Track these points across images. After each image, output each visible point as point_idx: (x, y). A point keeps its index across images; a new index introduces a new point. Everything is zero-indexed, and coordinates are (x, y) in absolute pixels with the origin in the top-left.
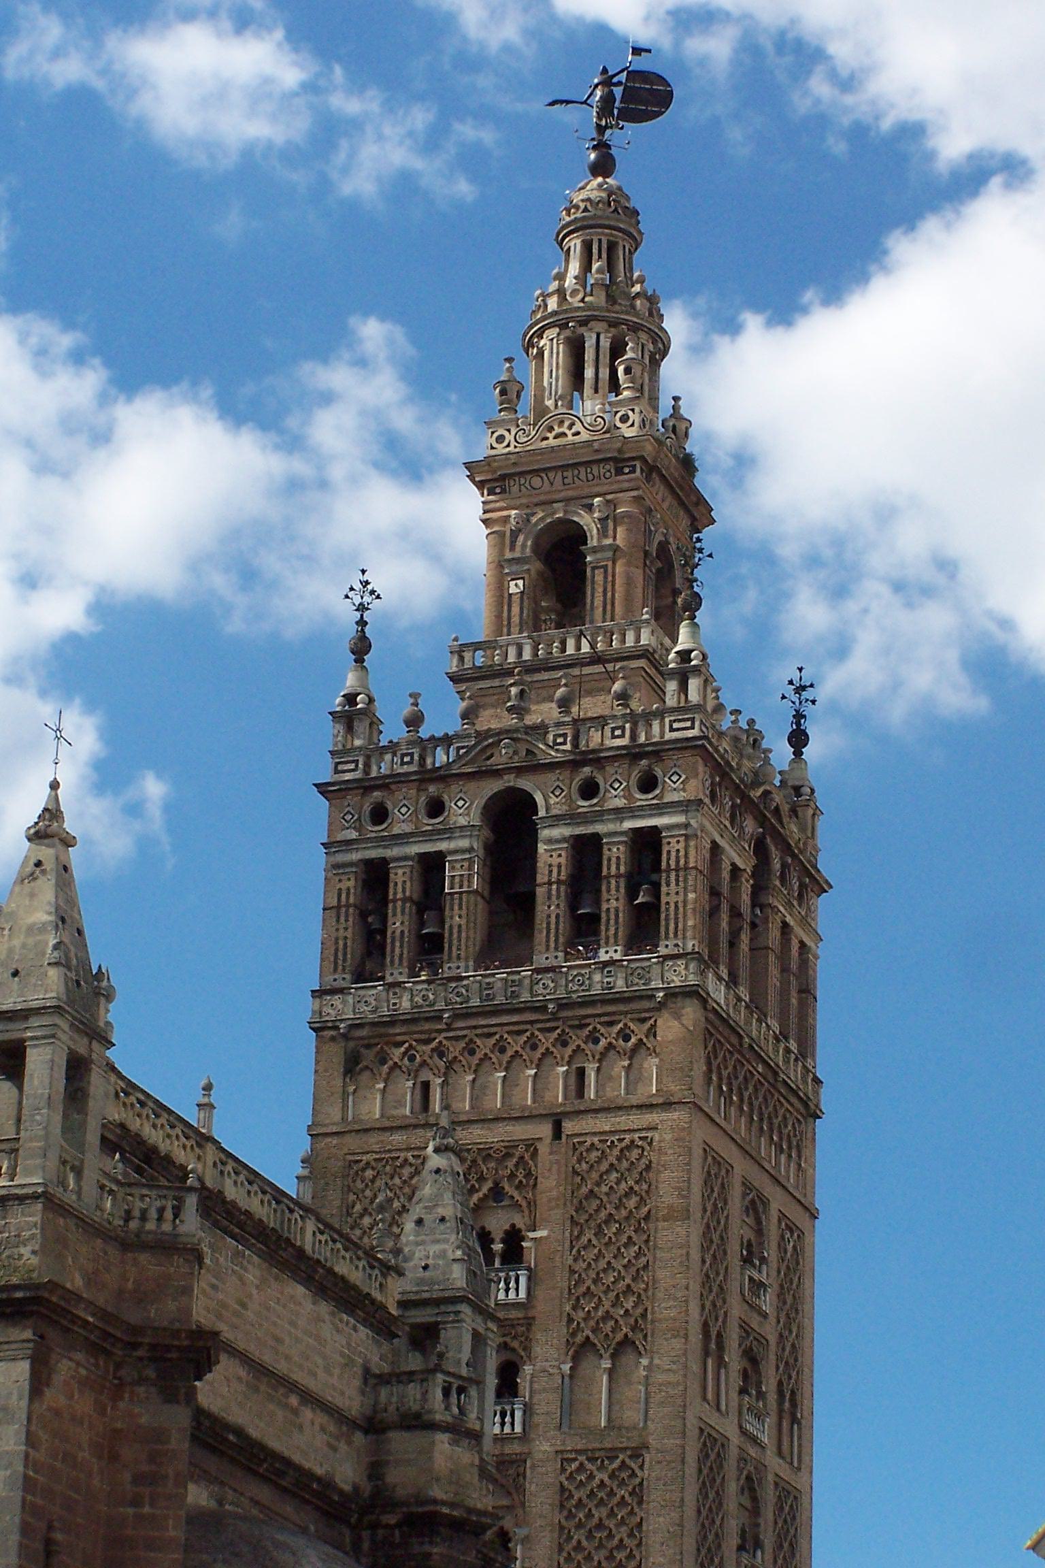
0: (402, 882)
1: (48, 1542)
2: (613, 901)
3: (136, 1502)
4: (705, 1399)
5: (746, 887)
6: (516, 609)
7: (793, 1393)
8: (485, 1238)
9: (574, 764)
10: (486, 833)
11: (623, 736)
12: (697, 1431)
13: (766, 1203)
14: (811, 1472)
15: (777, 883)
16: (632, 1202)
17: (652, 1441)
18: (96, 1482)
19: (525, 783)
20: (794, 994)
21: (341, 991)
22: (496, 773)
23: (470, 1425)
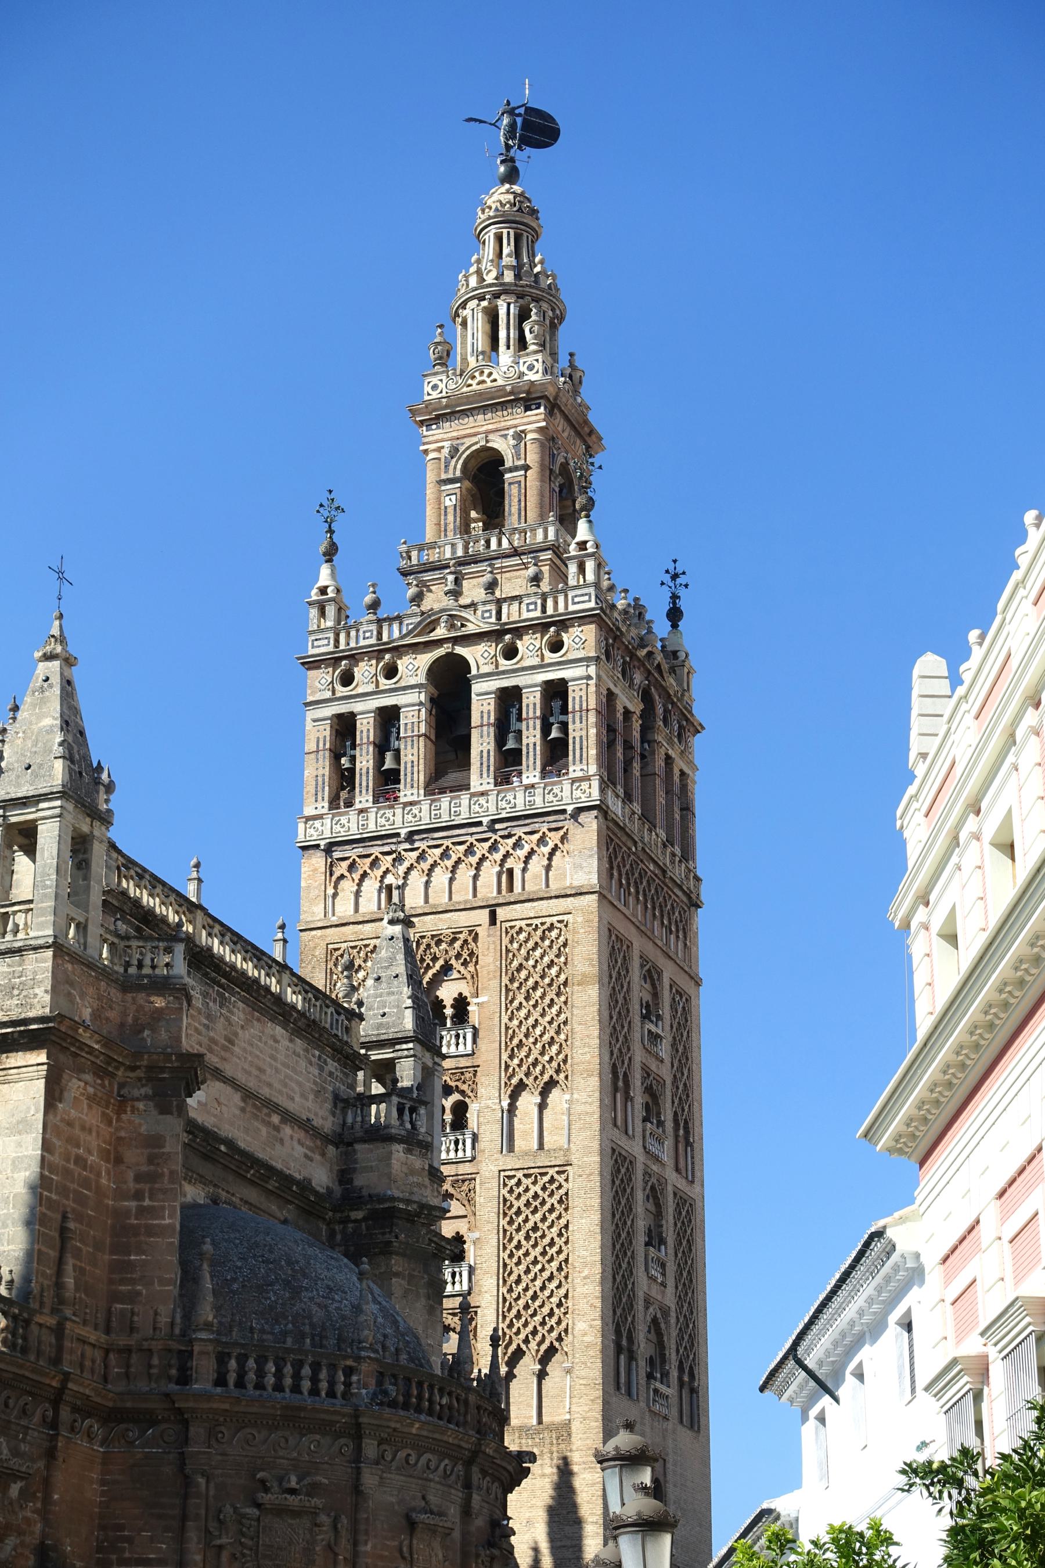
1: (63, 1231)
2: (532, 737)
3: (138, 1196)
4: (615, 1125)
5: (636, 725)
6: (450, 518)
7: (686, 1122)
8: (439, 1005)
10: (432, 689)
11: (536, 609)
12: (610, 1150)
13: (660, 974)
14: (703, 1186)
15: (661, 723)
16: (554, 971)
17: (574, 1159)
18: (104, 1181)
19: (459, 650)
20: (677, 810)
21: (320, 817)
22: (439, 643)
23: (421, 1137)
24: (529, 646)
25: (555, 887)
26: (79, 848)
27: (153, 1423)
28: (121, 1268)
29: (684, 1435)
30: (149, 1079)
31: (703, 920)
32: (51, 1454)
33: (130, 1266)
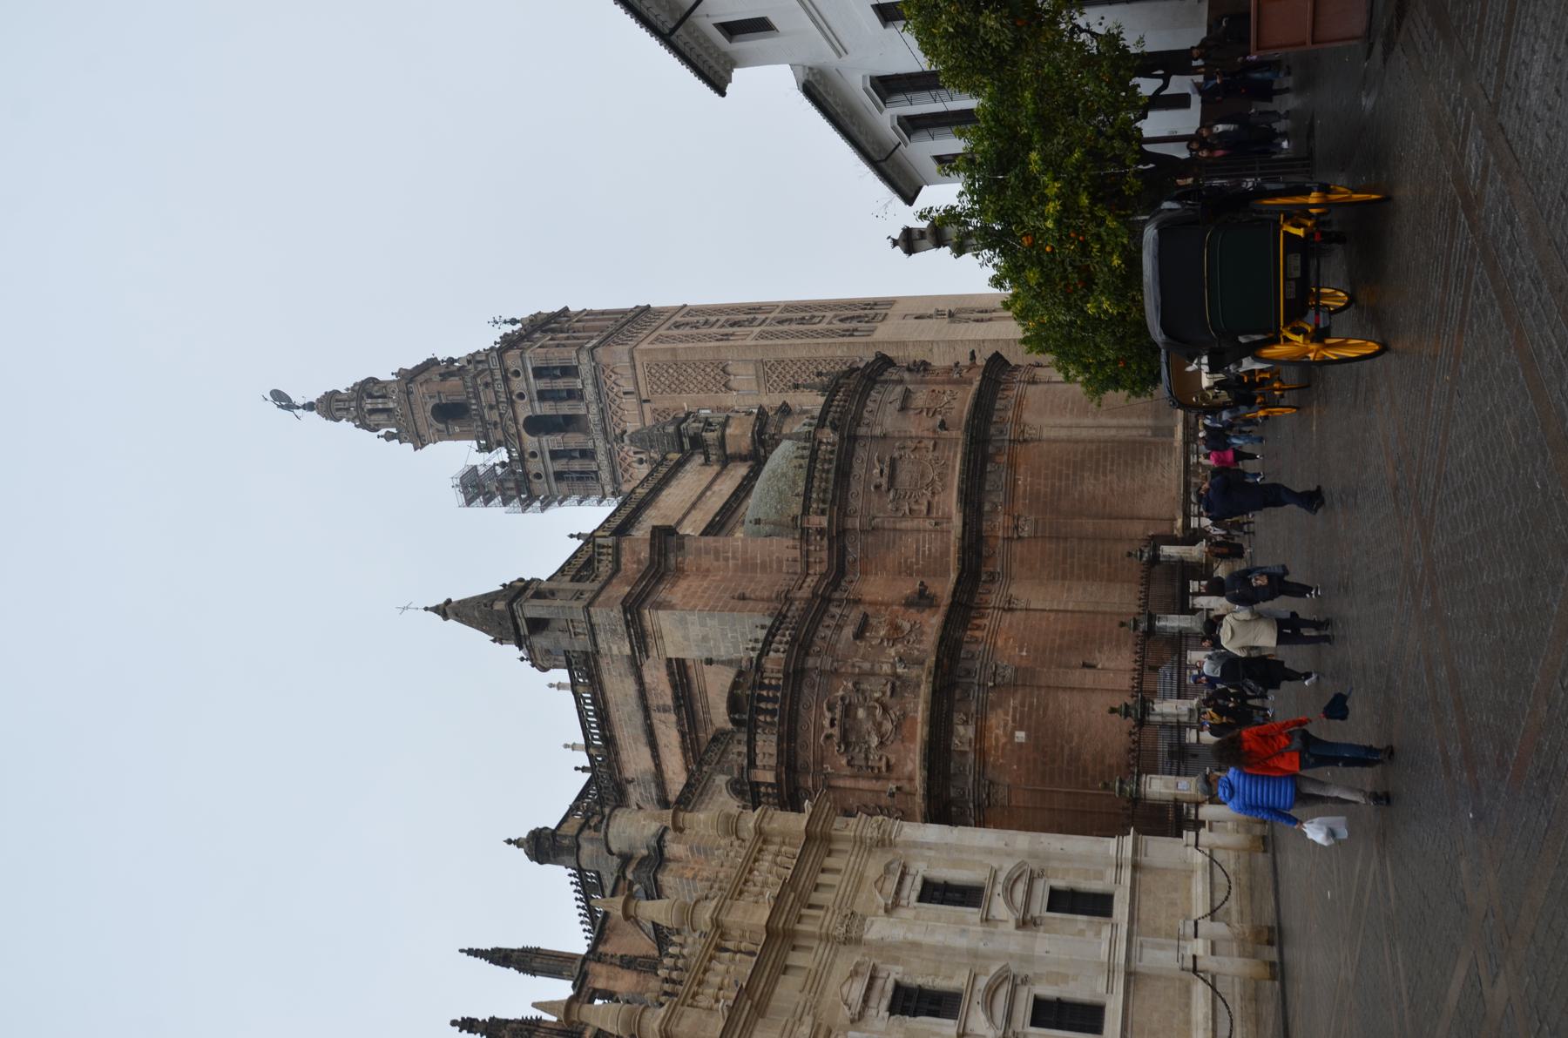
0: (560, 465)
2: (560, 384)
3: (726, 559)
9: (512, 403)
19: (521, 421)
26: (539, 595)
27: (845, 547)
28: (764, 566)
31: (656, 304)
32: (858, 602)
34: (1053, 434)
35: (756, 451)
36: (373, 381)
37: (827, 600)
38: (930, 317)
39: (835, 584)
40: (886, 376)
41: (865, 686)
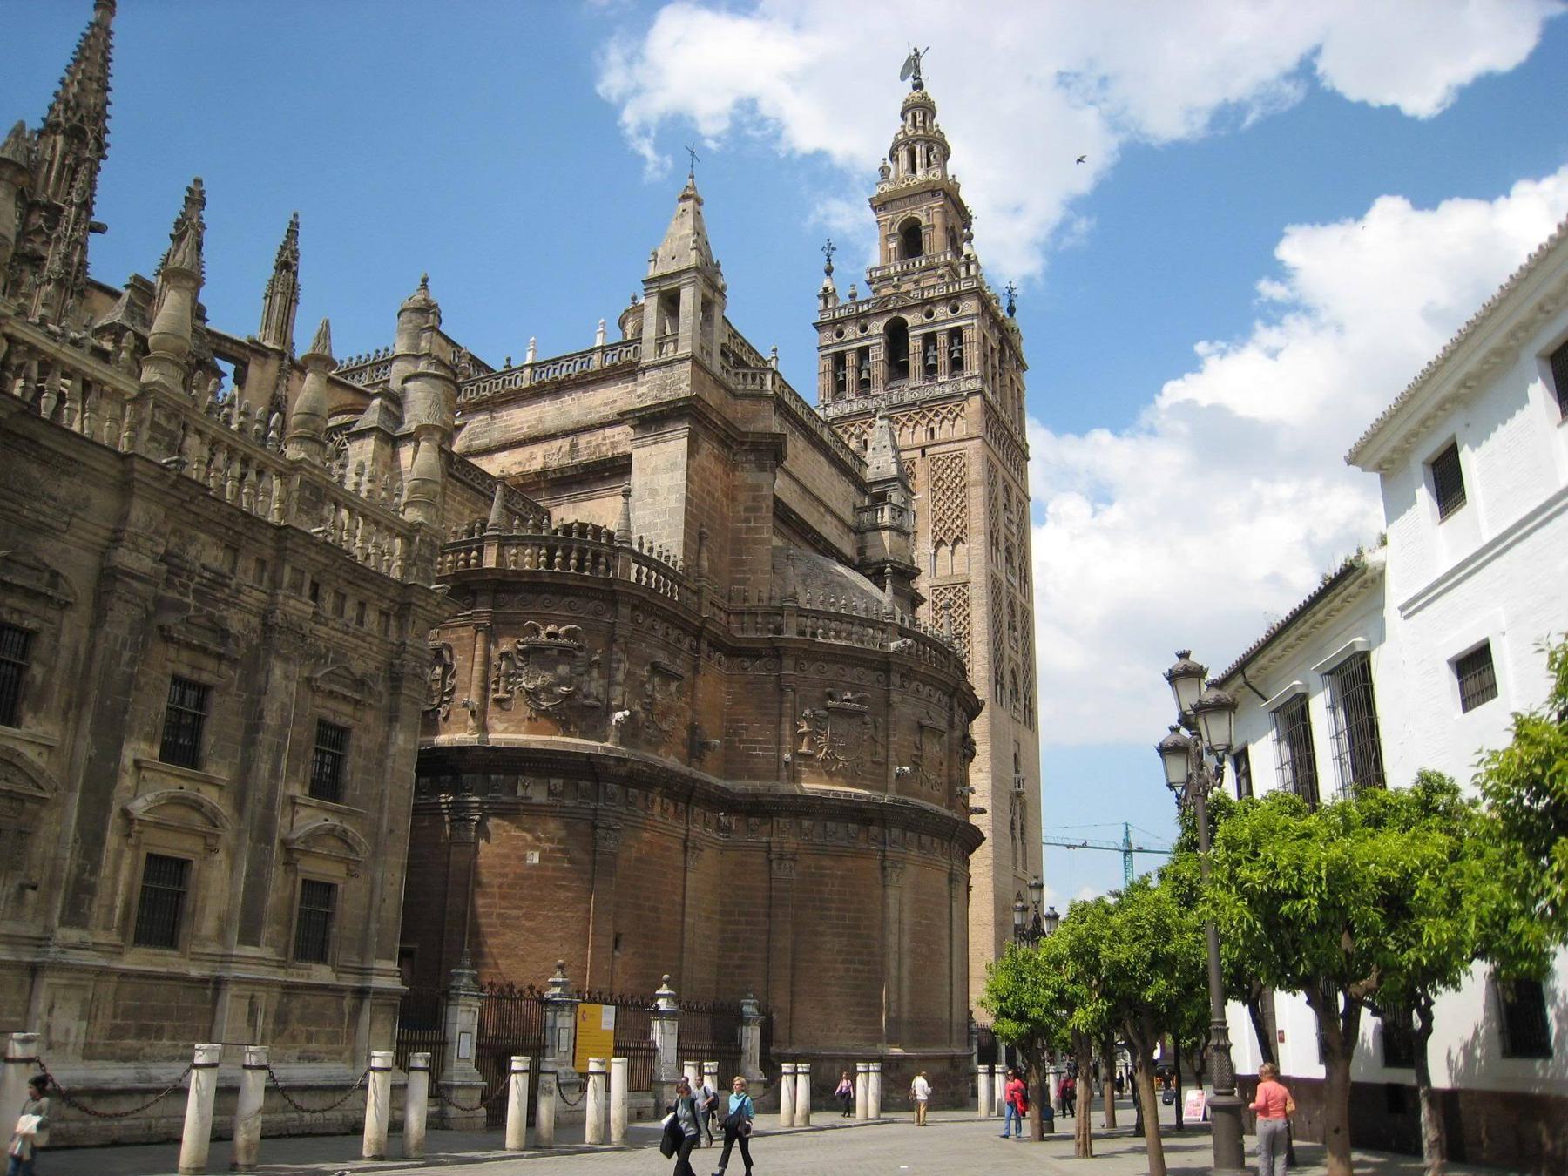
3: (747, 520)
19: (904, 316)
22: (890, 311)
24: (942, 312)
25: (957, 436)
26: (707, 306)
29: (1027, 732)
30: (752, 451)
32: (696, 670)
33: (742, 563)
34: (892, 902)
35: (869, 565)
36: (946, 155)
37: (698, 633)
38: (1017, 771)
39: (717, 645)
40: (958, 711)
41: (595, 673)
